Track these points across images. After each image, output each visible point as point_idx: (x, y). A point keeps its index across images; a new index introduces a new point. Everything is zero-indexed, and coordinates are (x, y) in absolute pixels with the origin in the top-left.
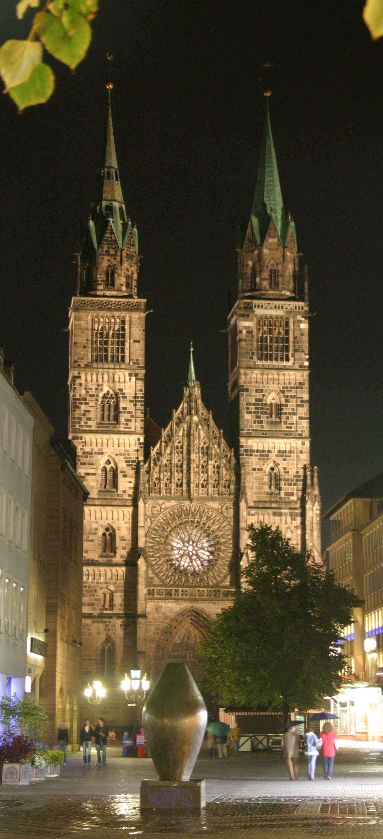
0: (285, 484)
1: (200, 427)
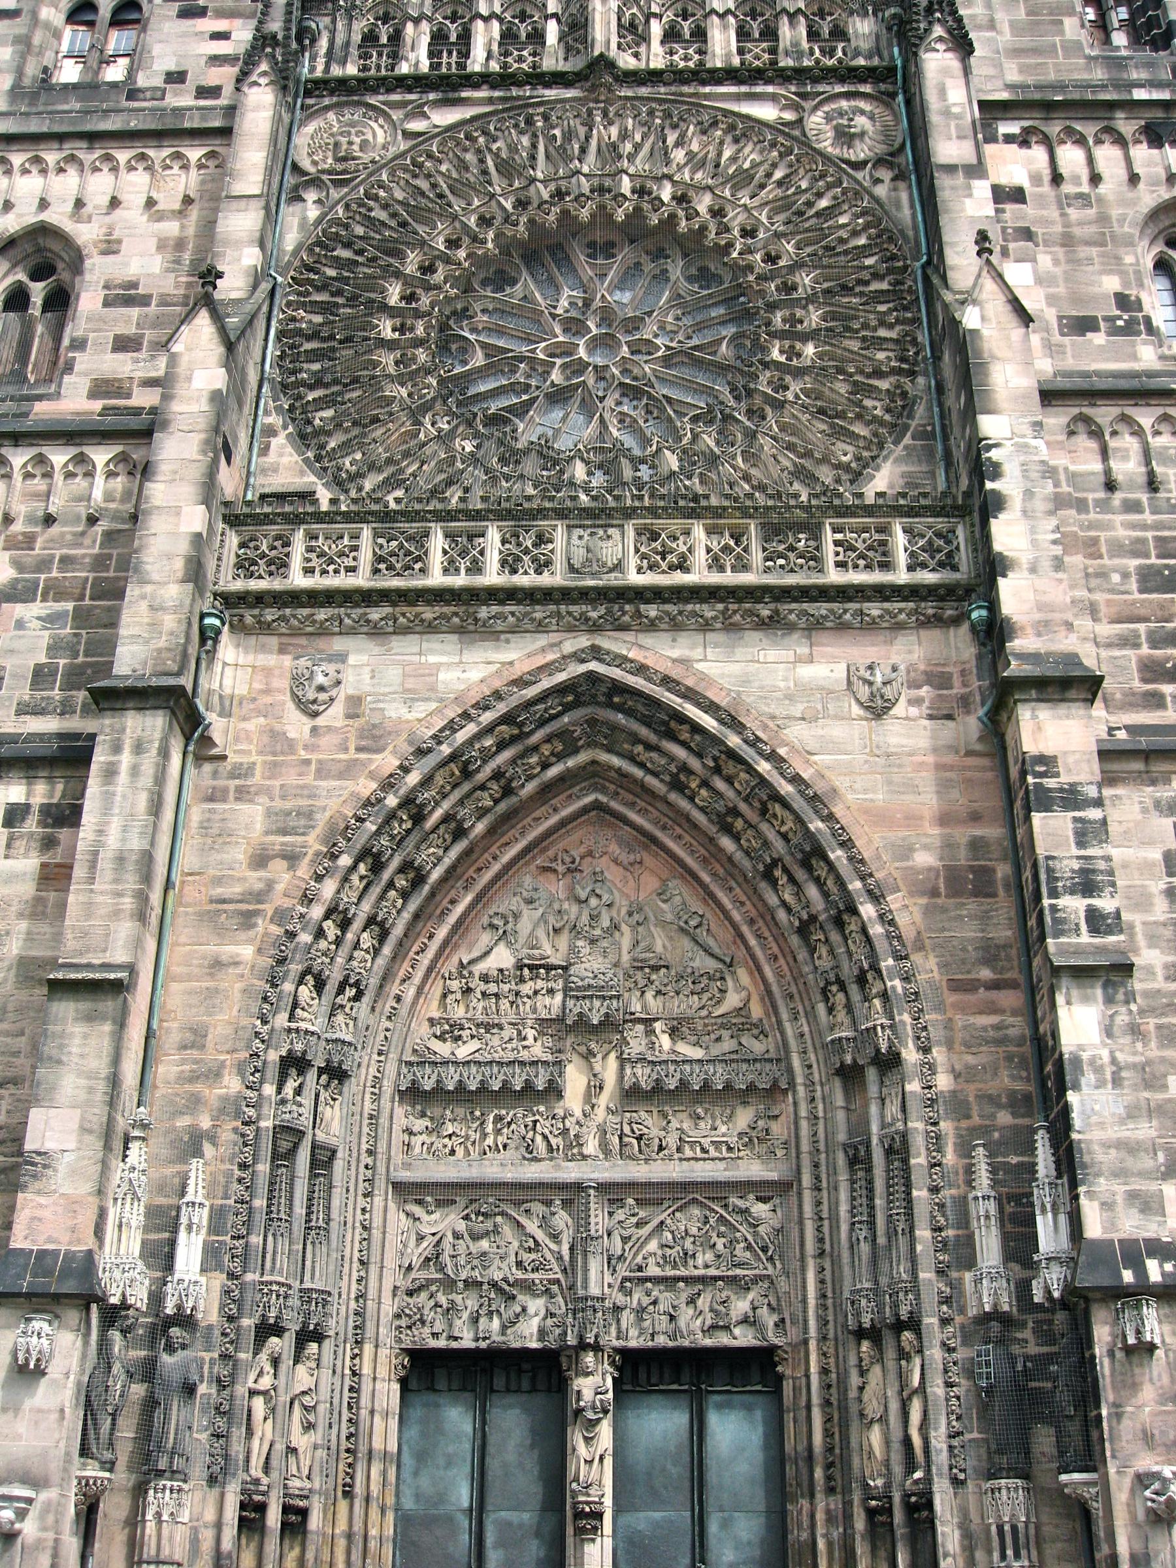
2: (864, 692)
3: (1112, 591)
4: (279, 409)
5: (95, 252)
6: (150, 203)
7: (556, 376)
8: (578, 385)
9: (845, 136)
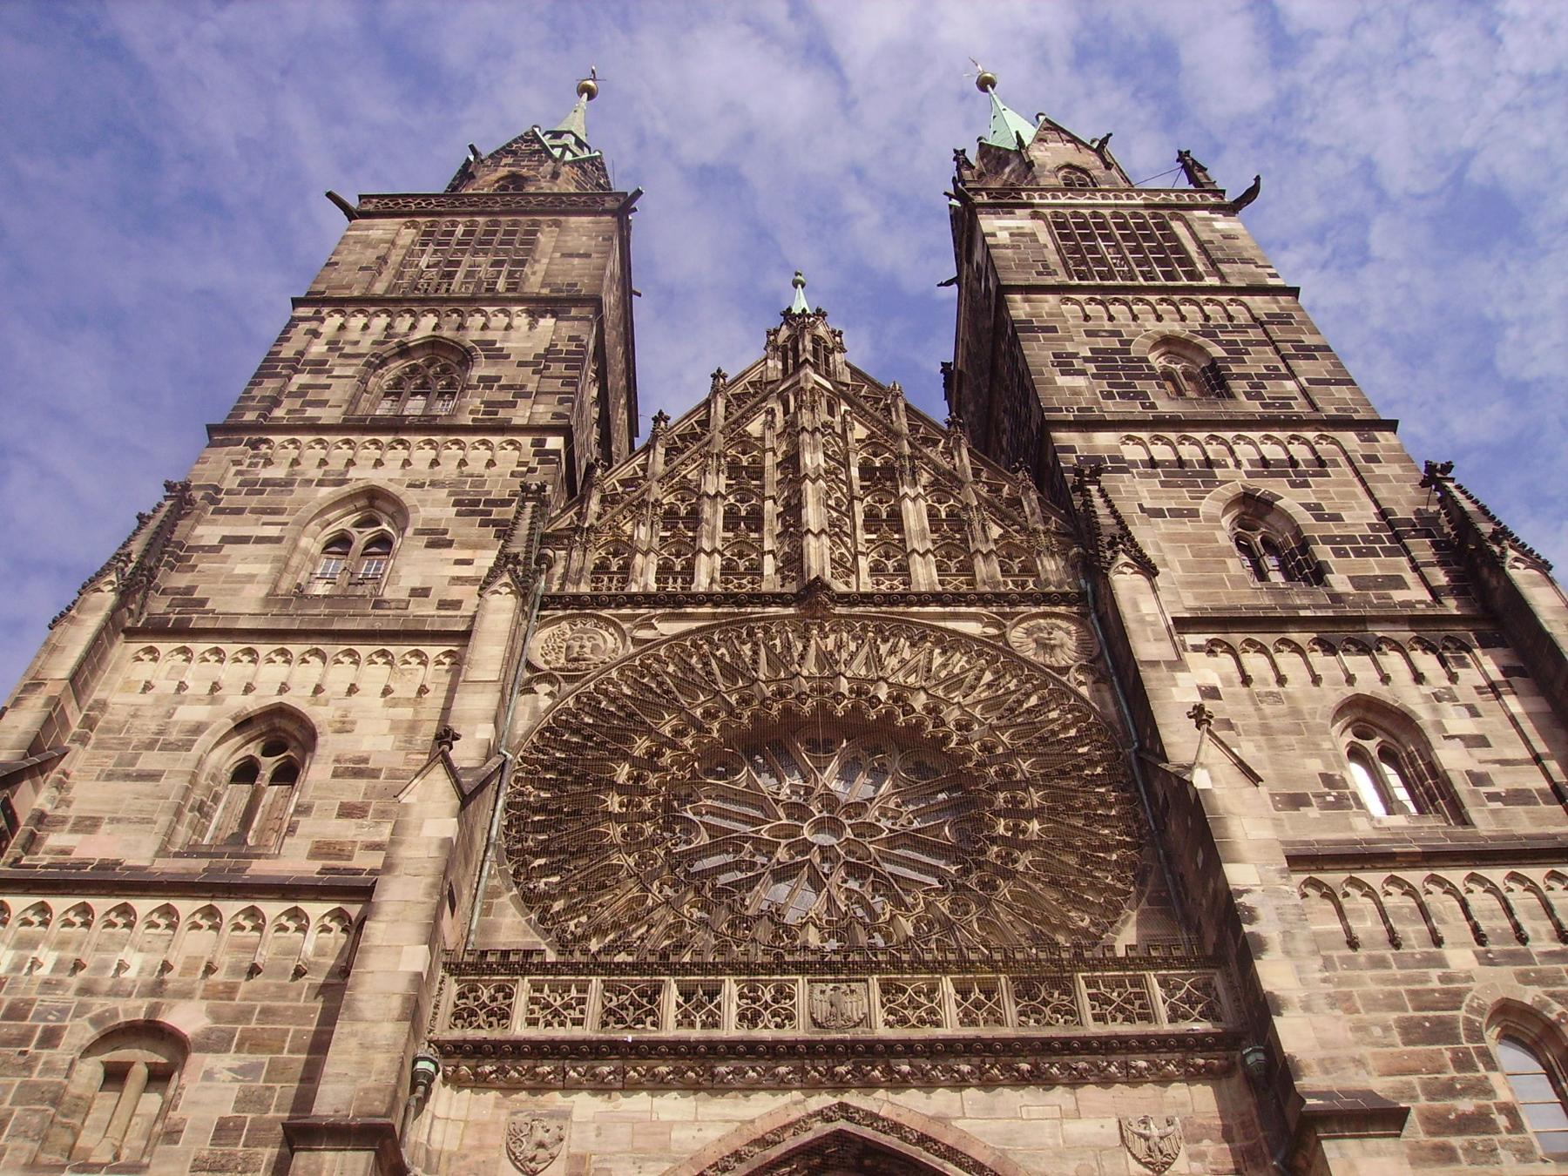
0: (1339, 553)
1: (844, 407)
2: (1140, 1147)
3: (1376, 1044)
4: (503, 873)
5: (329, 730)
6: (387, 691)
7: (782, 854)
8: (802, 865)
9: (1046, 647)
